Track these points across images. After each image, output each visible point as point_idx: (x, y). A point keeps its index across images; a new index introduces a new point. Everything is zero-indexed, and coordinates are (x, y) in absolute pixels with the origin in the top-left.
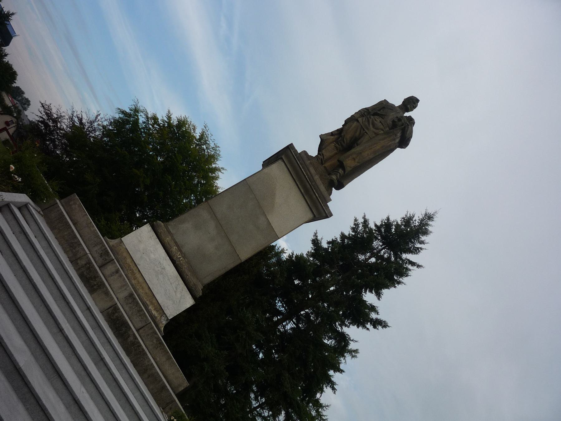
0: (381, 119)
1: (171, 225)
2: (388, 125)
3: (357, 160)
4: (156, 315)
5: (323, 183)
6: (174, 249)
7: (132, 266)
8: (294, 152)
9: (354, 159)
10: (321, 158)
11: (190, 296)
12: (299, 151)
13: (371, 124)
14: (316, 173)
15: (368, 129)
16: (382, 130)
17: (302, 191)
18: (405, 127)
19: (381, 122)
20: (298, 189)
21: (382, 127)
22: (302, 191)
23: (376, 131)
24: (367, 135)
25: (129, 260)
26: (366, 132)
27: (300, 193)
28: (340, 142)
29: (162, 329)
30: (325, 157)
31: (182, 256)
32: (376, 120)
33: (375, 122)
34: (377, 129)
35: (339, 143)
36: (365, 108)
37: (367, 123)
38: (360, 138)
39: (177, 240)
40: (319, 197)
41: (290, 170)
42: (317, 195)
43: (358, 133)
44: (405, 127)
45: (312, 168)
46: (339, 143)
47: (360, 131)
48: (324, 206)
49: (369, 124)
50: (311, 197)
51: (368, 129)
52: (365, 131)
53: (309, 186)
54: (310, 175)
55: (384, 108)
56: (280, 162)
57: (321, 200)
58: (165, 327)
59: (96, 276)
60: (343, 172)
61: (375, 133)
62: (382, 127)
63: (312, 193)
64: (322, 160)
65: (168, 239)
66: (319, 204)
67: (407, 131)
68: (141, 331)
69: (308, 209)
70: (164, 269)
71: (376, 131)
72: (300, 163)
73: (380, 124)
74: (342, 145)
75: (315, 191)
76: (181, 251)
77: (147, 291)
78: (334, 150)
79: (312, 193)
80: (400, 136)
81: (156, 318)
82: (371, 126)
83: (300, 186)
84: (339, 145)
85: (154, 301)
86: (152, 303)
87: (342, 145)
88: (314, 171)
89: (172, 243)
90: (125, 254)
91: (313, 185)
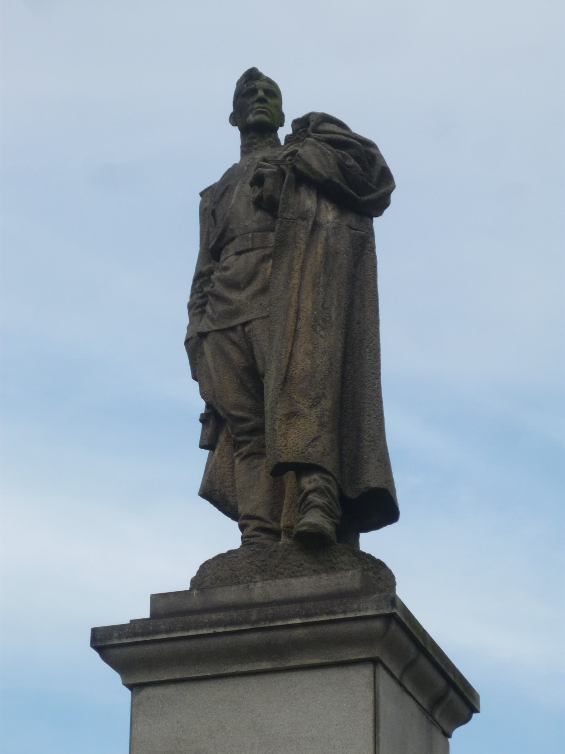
0: (232, 248)
2: (259, 231)
3: (303, 406)
5: (293, 575)
8: (120, 637)
9: (292, 415)
10: (256, 529)
12: (144, 613)
14: (241, 586)
15: (235, 313)
17: (265, 665)
18: (294, 169)
19: (239, 253)
20: (253, 680)
21: (253, 257)
22: (265, 665)
23: (256, 285)
24: (254, 323)
26: (244, 324)
27: (268, 679)
28: (238, 435)
30: (261, 512)
33: (228, 273)
34: (251, 278)
35: (240, 439)
36: (196, 279)
40: (308, 615)
41: (178, 676)
42: (298, 621)
43: (235, 355)
44: (294, 169)
45: (219, 590)
46: (240, 439)
47: (234, 343)
48: (344, 612)
49: (225, 300)
51: (235, 313)
52: (239, 328)
53: (255, 637)
54: (221, 616)
55: (213, 213)
57: (321, 615)
60: (316, 476)
62: (253, 257)
63: (284, 635)
66: (334, 628)
67: (307, 165)
69: (335, 674)
71: (256, 285)
72: (167, 632)
73: (243, 255)
75: (279, 623)
78: (256, 467)
79: (284, 635)
80: (314, 198)
82: (234, 296)
83: (246, 668)
84: (246, 442)
88: (234, 588)
91: (258, 621)
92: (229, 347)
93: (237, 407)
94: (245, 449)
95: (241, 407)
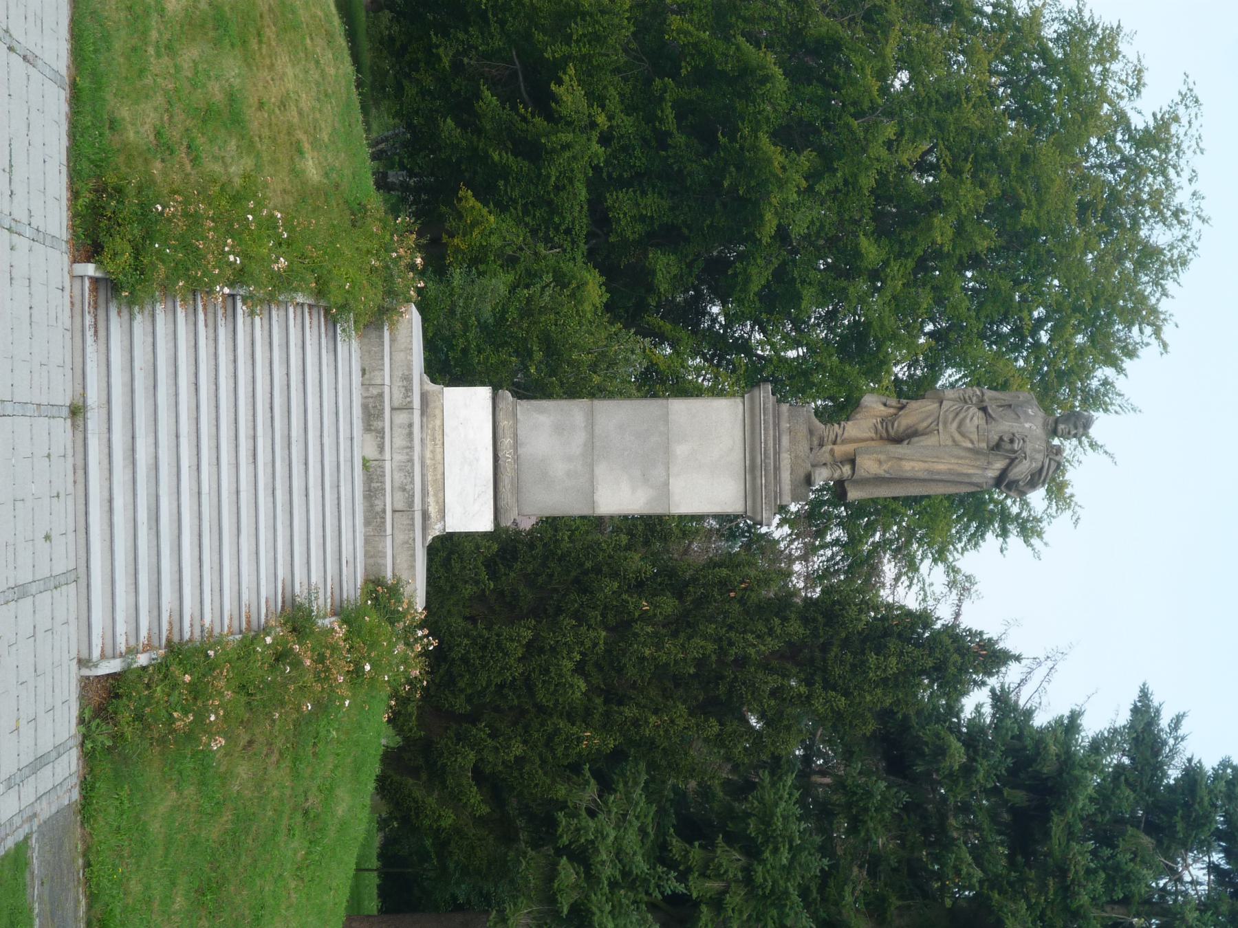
1: (524, 405)
3: (885, 467)
4: (432, 515)
6: (506, 442)
7: (438, 432)
9: (880, 462)
11: (492, 517)
13: (957, 420)
15: (945, 423)
16: (972, 442)
17: (747, 462)
21: (974, 437)
22: (747, 462)
25: (438, 422)
27: (743, 463)
29: (430, 538)
30: (846, 434)
31: (513, 458)
32: (972, 418)
34: (963, 435)
37: (951, 416)
38: (923, 434)
39: (519, 432)
43: (925, 424)
44: (1016, 458)
49: (954, 419)
50: (754, 479)
51: (945, 423)
56: (739, 400)
58: (435, 539)
59: (380, 415)
60: (850, 472)
61: (954, 441)
62: (974, 437)
63: (758, 474)
64: (836, 436)
65: (504, 423)
68: (397, 514)
70: (477, 460)
71: (958, 437)
74: (887, 431)
76: (516, 450)
77: (439, 476)
81: (429, 517)
82: (955, 425)
85: (441, 495)
86: (436, 495)
87: (887, 431)
89: (508, 433)
90: (438, 412)
92: (930, 420)
93: (899, 423)
94: (879, 426)
95: (898, 426)
